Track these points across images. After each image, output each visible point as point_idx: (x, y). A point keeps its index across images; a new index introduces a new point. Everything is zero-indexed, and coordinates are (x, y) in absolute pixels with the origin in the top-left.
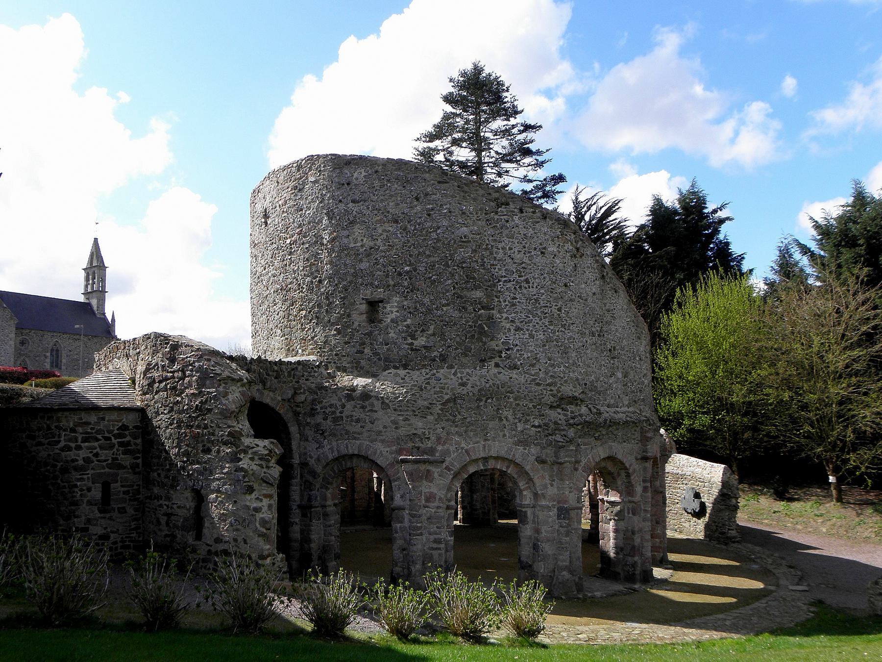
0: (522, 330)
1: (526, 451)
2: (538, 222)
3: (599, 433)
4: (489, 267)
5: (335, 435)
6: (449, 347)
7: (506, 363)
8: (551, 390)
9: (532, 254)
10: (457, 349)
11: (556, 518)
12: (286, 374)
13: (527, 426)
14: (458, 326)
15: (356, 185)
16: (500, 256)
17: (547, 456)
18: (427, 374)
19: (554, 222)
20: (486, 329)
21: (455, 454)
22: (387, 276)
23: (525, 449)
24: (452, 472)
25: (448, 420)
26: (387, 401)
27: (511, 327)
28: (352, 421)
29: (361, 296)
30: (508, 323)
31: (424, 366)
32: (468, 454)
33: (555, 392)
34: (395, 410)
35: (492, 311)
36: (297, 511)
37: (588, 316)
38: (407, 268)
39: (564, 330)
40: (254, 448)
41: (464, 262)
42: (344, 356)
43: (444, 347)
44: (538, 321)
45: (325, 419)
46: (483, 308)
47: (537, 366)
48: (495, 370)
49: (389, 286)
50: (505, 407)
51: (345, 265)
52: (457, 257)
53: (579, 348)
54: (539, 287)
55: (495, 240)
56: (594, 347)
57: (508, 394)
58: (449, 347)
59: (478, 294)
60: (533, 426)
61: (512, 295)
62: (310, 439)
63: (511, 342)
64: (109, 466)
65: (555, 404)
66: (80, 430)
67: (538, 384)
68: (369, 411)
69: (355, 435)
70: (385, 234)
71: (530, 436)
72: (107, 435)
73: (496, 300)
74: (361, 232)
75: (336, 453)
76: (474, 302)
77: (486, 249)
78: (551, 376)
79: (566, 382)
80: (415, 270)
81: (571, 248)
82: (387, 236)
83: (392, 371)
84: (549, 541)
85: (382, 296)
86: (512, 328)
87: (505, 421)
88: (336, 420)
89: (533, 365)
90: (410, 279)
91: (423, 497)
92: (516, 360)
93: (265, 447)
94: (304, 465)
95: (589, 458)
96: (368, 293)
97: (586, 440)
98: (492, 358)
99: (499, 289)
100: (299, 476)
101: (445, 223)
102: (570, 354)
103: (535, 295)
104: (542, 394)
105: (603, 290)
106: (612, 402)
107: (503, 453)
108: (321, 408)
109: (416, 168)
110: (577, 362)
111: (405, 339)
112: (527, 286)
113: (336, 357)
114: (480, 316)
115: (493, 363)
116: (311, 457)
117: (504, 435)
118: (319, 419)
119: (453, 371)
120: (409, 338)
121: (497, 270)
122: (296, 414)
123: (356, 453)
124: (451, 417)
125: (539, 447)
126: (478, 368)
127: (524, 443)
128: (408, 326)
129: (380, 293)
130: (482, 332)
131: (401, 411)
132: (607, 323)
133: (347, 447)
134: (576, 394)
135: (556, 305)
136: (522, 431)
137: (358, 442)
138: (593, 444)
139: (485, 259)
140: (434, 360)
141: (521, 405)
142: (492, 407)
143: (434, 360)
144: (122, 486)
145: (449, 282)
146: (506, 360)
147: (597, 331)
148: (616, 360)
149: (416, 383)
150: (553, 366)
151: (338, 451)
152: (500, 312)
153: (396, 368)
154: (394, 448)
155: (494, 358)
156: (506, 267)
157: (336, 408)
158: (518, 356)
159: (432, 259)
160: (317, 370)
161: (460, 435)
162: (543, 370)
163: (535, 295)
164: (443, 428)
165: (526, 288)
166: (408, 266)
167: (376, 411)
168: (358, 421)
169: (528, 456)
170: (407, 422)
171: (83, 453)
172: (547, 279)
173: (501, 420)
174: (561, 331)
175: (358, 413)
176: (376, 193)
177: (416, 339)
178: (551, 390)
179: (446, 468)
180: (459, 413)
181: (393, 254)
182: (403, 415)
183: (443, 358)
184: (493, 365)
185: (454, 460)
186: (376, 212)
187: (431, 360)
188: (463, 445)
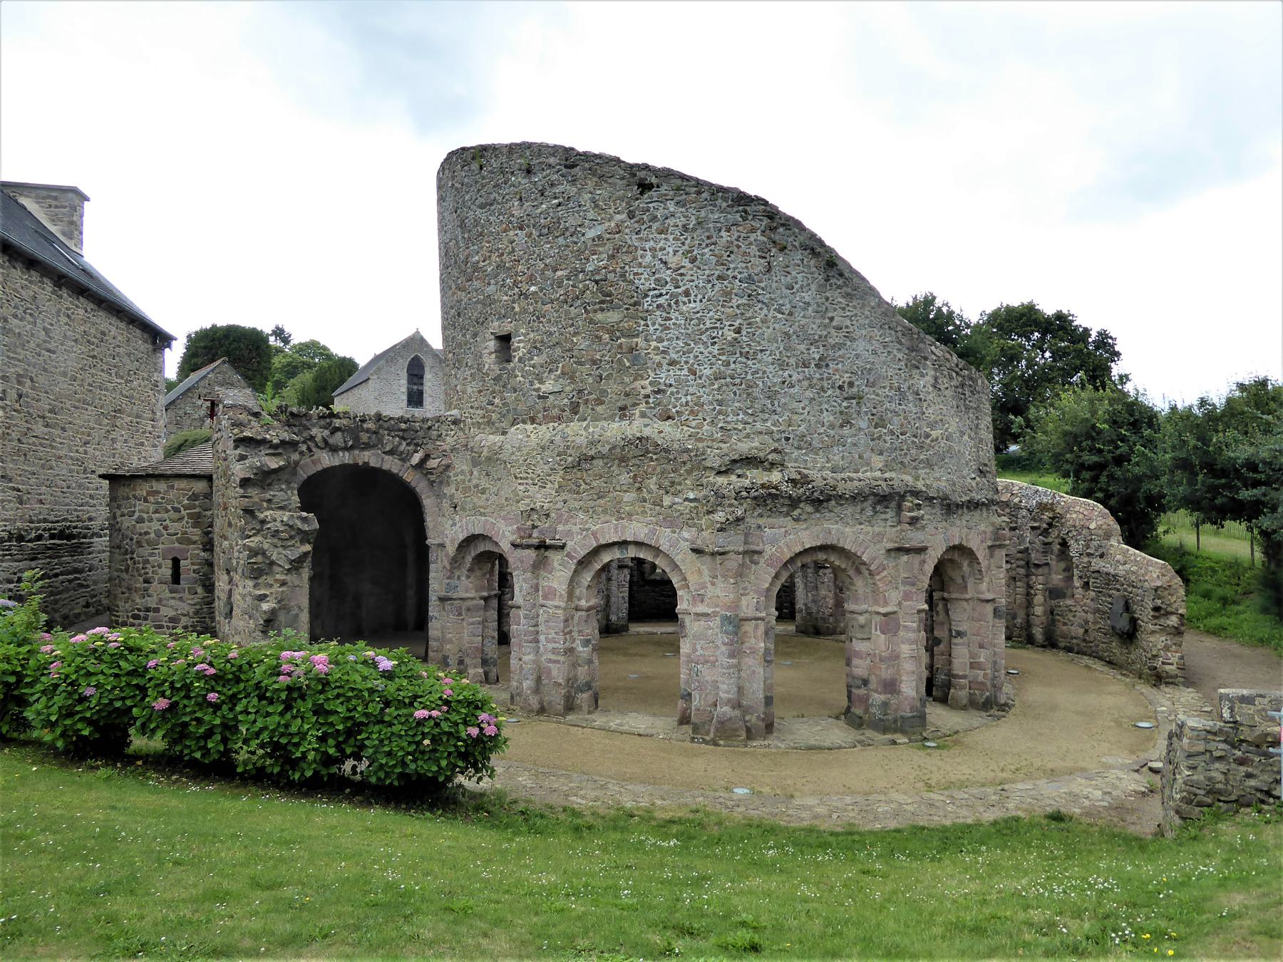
1: (676, 535)
4: (632, 277)
9: (695, 253)
19: (730, 202)
34: (516, 477)
35: (635, 340)
36: (438, 603)
37: (795, 337)
39: (744, 360)
41: (598, 273)
44: (702, 350)
46: (623, 336)
56: (806, 383)
60: (686, 499)
65: (724, 469)
66: (151, 499)
67: (700, 440)
69: (482, 510)
72: (176, 505)
73: (642, 323)
78: (721, 428)
86: (664, 362)
91: (540, 593)
96: (496, 326)
98: (635, 405)
99: (646, 306)
112: (686, 299)
114: (620, 346)
115: (637, 412)
121: (643, 281)
129: (507, 327)
131: (521, 478)
135: (730, 325)
136: (670, 507)
138: (789, 527)
139: (627, 267)
144: (192, 564)
147: (814, 359)
152: (646, 340)
153: (524, 422)
156: (657, 276)
165: (684, 303)
171: (156, 526)
172: (717, 288)
175: (484, 483)
184: (638, 415)
185: (579, 546)
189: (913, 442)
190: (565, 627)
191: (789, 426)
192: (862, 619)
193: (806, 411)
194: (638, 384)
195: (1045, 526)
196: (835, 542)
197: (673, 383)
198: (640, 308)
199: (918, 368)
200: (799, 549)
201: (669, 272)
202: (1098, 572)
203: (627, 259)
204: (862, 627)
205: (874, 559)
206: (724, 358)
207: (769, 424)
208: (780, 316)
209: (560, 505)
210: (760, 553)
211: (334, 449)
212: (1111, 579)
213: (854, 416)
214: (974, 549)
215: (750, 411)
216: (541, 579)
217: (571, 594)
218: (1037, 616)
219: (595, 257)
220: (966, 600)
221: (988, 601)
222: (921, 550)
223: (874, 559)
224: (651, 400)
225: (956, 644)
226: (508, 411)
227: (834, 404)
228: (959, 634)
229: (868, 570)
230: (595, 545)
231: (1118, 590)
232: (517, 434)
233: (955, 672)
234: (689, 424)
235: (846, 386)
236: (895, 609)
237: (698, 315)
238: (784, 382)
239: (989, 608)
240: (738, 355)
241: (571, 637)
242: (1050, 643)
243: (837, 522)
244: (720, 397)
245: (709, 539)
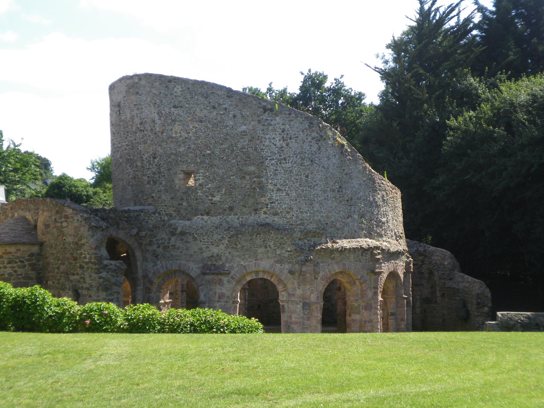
0: (282, 190)
1: (282, 267)
2: (292, 120)
4: (260, 151)
5: (164, 258)
8: (300, 228)
11: (301, 309)
13: (283, 251)
15: (175, 96)
16: (267, 143)
18: (221, 219)
19: (304, 119)
22: (196, 156)
23: (281, 265)
25: (233, 248)
26: (196, 236)
28: (175, 248)
29: (180, 169)
31: (219, 214)
32: (246, 269)
33: (303, 229)
34: (201, 241)
35: (262, 179)
37: (329, 179)
38: (208, 152)
39: (309, 189)
40: (109, 266)
41: (244, 148)
42: (170, 207)
44: (292, 184)
45: (158, 247)
47: (291, 214)
49: (197, 163)
50: (269, 239)
51: (170, 148)
52: (240, 145)
53: (322, 201)
54: (293, 163)
55: (264, 134)
56: (334, 199)
59: (252, 168)
60: (287, 251)
61: (275, 168)
62: (149, 260)
63: (274, 198)
64: (23, 278)
68: (185, 242)
69: (177, 258)
70: (194, 129)
72: (21, 259)
73: (265, 171)
74: (179, 127)
75: (165, 269)
76: (249, 174)
77: (258, 139)
79: (311, 222)
80: (213, 153)
81: (316, 135)
82: (195, 130)
83: (200, 216)
85: (193, 169)
86: (275, 190)
87: (268, 248)
88: (165, 248)
89: (288, 213)
90: (210, 159)
93: (115, 265)
94: (145, 276)
98: (262, 208)
99: (266, 164)
100: (142, 285)
101: (231, 123)
102: (314, 205)
103: (290, 168)
105: (342, 161)
108: (156, 240)
109: (213, 87)
110: (320, 209)
111: (207, 196)
112: (284, 162)
113: (165, 207)
114: (254, 182)
116: (150, 272)
118: (155, 247)
119: (237, 217)
120: (210, 196)
121: (265, 152)
122: (140, 244)
123: (177, 269)
124: (234, 246)
126: (253, 215)
127: (281, 262)
128: (209, 189)
132: (345, 182)
133: (172, 265)
135: (304, 174)
137: (178, 262)
142: (260, 239)
145: (234, 161)
146: (271, 210)
147: (337, 188)
149: (214, 224)
150: (302, 212)
151: (167, 268)
152: (267, 180)
153: (202, 215)
154: (200, 265)
157: (166, 241)
158: (279, 207)
159: (223, 146)
160: (153, 215)
161: (240, 257)
163: (290, 168)
164: (230, 253)
166: (209, 150)
167: (189, 242)
168: (178, 248)
170: (208, 249)
173: (266, 247)
174: (308, 190)
176: (188, 102)
177: (214, 197)
179: (231, 278)
180: (239, 243)
181: (199, 142)
182: (205, 245)
183: (231, 209)
186: (188, 115)
187: (224, 210)
194: (263, 199)
195: (420, 263)
198: (264, 165)
200: (333, 273)
201: (277, 149)
203: (258, 142)
206: (301, 188)
208: (323, 169)
209: (227, 254)
213: (353, 213)
219: (242, 140)
224: (269, 206)
226: (192, 209)
232: (198, 219)
235: (349, 200)
237: (290, 169)
240: (307, 187)
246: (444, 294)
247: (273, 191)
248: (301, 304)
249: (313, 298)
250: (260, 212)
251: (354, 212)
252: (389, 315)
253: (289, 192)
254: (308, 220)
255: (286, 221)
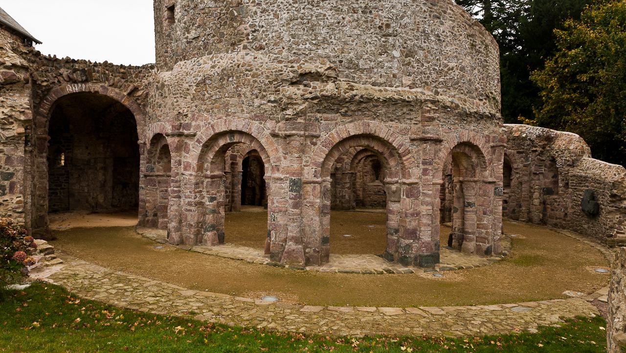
0: (268, 11)
1: (262, 125)
3: (346, 109)
6: (208, 35)
7: (253, 44)
10: (214, 36)
11: (287, 190)
12: (134, 76)
13: (263, 102)
14: (214, 15)
17: (279, 130)
20: (236, 14)
21: (204, 129)
24: (201, 145)
27: (257, 10)
30: (254, 6)
33: (296, 68)
39: (311, 7)
43: (205, 37)
48: (243, 52)
50: (243, 84)
56: (355, 24)
57: (247, 72)
58: (208, 35)
60: (269, 101)
63: (257, 24)
65: (294, 80)
67: (280, 62)
71: (266, 111)
78: (294, 53)
79: (311, 59)
84: (281, 211)
87: (243, 98)
91: (182, 166)
92: (262, 41)
95: (332, 134)
97: (329, 116)
98: (240, 41)
104: (282, 71)
106: (382, 80)
107: (240, 128)
110: (328, 38)
115: (241, 46)
117: (243, 111)
124: (201, 96)
125: (274, 121)
126: (230, 52)
127: (261, 117)
130: (233, 18)
134: (321, 70)
136: (259, 107)
138: (339, 120)
140: (200, 49)
141: (258, 81)
142: (233, 85)
143: (200, 49)
146: (253, 42)
147: (361, 7)
148: (391, 39)
155: (242, 40)
158: (264, 36)
162: (286, 48)
164: (196, 106)
169: (262, 131)
173: (239, 95)
178: (292, 67)
184: (242, 48)
188: (209, 121)
189: (434, 69)
190: (196, 188)
191: (342, 53)
192: (394, 187)
193: (354, 43)
194: (242, 27)
196: (373, 132)
197: (264, 25)
199: (439, 18)
200: (345, 136)
202: (574, 176)
204: (394, 192)
205: (401, 145)
206: (296, 5)
207: (327, 51)
210: (317, 137)
211: (74, 82)
212: (583, 179)
214: (480, 147)
215: (314, 42)
216: (183, 157)
217: (200, 168)
218: (535, 205)
220: (475, 182)
221: (490, 183)
222: (438, 141)
223: (401, 145)
224: (250, 37)
225: (467, 211)
227: (376, 39)
228: (469, 204)
229: (398, 153)
230: (213, 133)
231: (588, 187)
233: (466, 230)
234: (273, 51)
235: (384, 27)
236: (416, 181)
238: (339, 23)
239: (491, 188)
241: (201, 195)
242: (543, 222)
243: (374, 119)
244: (293, 32)
245: (281, 128)
246: (567, 184)
247: (256, 13)
248: (288, 182)
249: (309, 174)
250: (239, 46)
251: (394, 46)
252: (465, 206)
253: (278, 12)
254: (307, 55)
255: (273, 58)
